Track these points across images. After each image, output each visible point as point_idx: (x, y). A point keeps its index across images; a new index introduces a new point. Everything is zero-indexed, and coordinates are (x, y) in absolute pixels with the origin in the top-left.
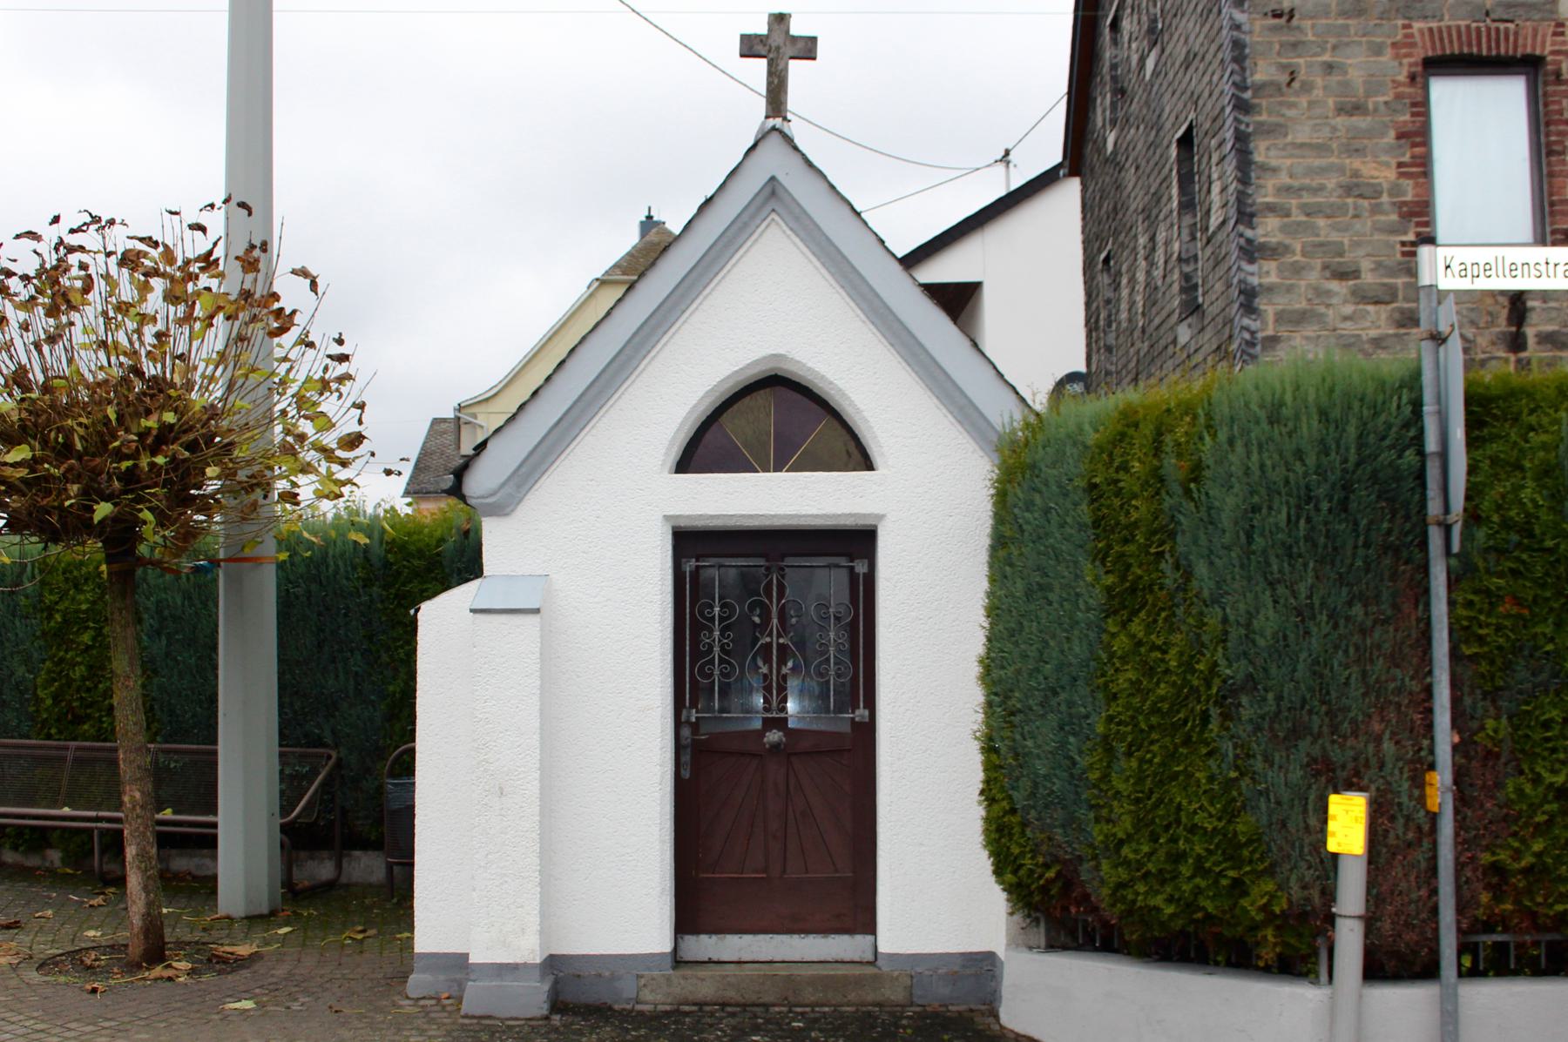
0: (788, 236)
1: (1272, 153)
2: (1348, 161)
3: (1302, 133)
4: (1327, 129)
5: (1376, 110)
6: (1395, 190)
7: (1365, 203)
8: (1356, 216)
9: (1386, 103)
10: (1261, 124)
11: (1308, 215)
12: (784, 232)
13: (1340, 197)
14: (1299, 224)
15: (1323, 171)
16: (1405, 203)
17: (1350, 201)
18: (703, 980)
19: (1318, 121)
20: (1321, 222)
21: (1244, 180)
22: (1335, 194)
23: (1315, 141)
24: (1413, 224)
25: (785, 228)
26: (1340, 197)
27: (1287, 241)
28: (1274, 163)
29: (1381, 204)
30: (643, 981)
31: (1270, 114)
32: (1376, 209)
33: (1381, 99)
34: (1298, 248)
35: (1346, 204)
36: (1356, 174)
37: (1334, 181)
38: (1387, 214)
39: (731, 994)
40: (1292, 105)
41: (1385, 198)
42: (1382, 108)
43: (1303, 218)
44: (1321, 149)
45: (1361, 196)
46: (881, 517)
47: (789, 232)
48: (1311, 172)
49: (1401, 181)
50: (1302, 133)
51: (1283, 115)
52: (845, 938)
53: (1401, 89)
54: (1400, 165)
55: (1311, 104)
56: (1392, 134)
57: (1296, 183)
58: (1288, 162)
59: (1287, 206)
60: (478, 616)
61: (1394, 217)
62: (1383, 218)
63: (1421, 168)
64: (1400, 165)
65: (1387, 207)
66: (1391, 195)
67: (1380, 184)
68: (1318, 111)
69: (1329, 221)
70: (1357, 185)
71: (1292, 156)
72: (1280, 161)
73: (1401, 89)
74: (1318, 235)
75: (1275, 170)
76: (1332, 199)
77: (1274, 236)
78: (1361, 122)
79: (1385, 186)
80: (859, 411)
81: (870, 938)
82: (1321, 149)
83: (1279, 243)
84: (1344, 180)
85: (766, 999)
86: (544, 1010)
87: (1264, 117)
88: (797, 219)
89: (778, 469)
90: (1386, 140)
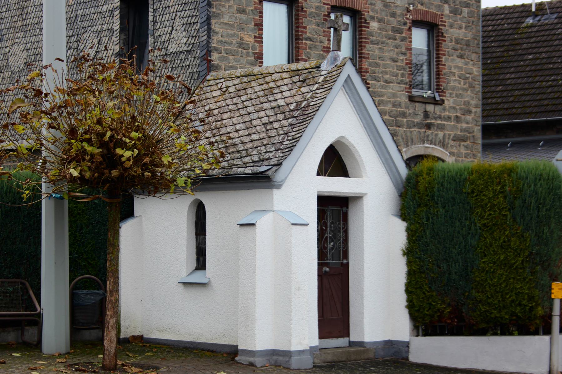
0: (345, 95)
1: (217, 25)
2: (240, 33)
3: (226, 19)
4: (234, 19)
5: (249, 13)
6: (253, 48)
7: (244, 51)
8: (242, 56)
9: (252, 10)
10: (214, 12)
11: (227, 54)
12: (344, 93)
13: (237, 47)
14: (224, 57)
15: (233, 35)
16: (256, 53)
17: (240, 49)
18: (329, 354)
19: (231, 14)
20: (231, 57)
21: (209, 37)
22: (236, 46)
23: (230, 23)
24: (258, 62)
25: (345, 92)
26: (237, 47)
27: (220, 64)
28: (217, 30)
29: (249, 52)
30: (315, 356)
31: (216, 8)
32: (248, 55)
33: (251, 8)
34: (223, 67)
35: (238, 51)
36: (242, 39)
37: (235, 40)
38: (251, 57)
39: (335, 359)
40: (224, 6)
41: (250, 50)
42: (251, 12)
43: (225, 55)
44: (231, 26)
45: (244, 48)
46: (366, 194)
47: (346, 93)
48: (229, 35)
49: (255, 44)
50: (226, 19)
51: (220, 10)
52: (342, 339)
53: (256, 5)
54: (255, 37)
55: (229, 6)
56: (253, 23)
57: (224, 40)
58: (221, 30)
59: (220, 49)
60: (294, 226)
61: (253, 58)
62: (250, 58)
63: (259, 39)
64: (255, 37)
65: (251, 54)
66: (252, 49)
67: (248, 44)
68: (231, 10)
69: (234, 57)
70: (242, 44)
71: (222, 28)
72: (219, 29)
73: (256, 5)
74: (230, 63)
75: (217, 33)
76: (235, 48)
77: (216, 61)
78: (244, 17)
79: (251, 45)
80: (361, 158)
81: (348, 338)
82: (231, 26)
83: (218, 64)
84: (238, 40)
85: (344, 359)
86: (311, 366)
87: (214, 10)
88: (350, 90)
89: (325, 176)
90: (251, 26)
